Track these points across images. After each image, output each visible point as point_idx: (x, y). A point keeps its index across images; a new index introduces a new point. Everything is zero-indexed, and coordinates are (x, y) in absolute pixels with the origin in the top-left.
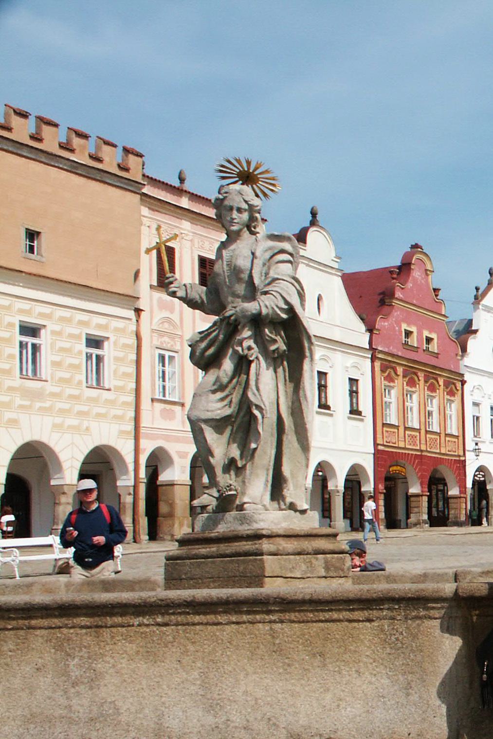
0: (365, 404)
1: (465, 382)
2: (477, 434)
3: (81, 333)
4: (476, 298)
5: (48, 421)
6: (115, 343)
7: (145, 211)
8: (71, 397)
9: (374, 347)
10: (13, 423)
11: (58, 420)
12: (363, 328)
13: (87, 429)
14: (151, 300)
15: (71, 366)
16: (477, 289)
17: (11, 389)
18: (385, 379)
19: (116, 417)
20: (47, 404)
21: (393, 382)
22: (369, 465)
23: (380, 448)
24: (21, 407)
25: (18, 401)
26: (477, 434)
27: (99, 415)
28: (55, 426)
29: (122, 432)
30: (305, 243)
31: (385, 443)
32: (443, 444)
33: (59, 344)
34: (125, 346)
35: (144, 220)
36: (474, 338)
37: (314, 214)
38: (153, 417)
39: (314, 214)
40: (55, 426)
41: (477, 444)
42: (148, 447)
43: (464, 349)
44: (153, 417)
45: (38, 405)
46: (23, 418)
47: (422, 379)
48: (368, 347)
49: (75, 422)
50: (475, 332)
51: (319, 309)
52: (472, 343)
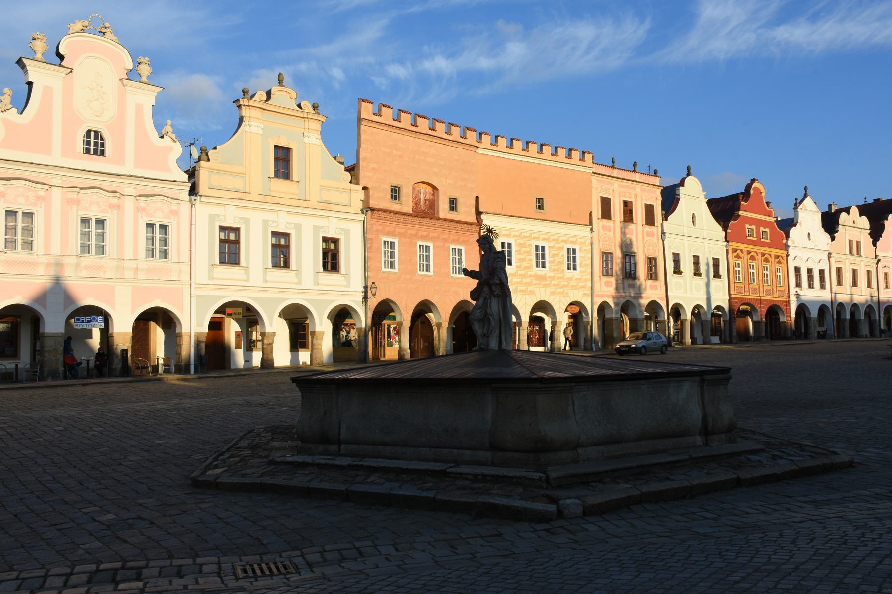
0: (723, 270)
1: (789, 255)
2: (798, 284)
3: (563, 246)
4: (796, 205)
5: (548, 290)
6: (580, 250)
7: (594, 179)
8: (559, 278)
9: (728, 240)
10: (532, 292)
11: (553, 290)
12: (720, 228)
13: (567, 293)
14: (598, 224)
15: (559, 263)
16: (796, 200)
17: (531, 276)
18: (735, 257)
19: (582, 287)
20: (548, 282)
21: (741, 258)
22: (726, 306)
23: (733, 296)
24: (535, 284)
25: (534, 282)
26: (798, 284)
27: (573, 286)
28: (551, 292)
29: (584, 294)
30: (684, 186)
31: (736, 293)
32: (775, 293)
33: (553, 252)
34: (585, 250)
35: (594, 186)
36: (796, 229)
37: (689, 169)
38: (601, 286)
39: (689, 169)
40: (551, 292)
41: (797, 291)
42: (598, 301)
43: (788, 236)
44: (601, 286)
45: (543, 283)
46: (537, 290)
47: (760, 256)
48: (724, 240)
49: (561, 290)
50: (795, 225)
51: (693, 222)
52: (793, 231)
